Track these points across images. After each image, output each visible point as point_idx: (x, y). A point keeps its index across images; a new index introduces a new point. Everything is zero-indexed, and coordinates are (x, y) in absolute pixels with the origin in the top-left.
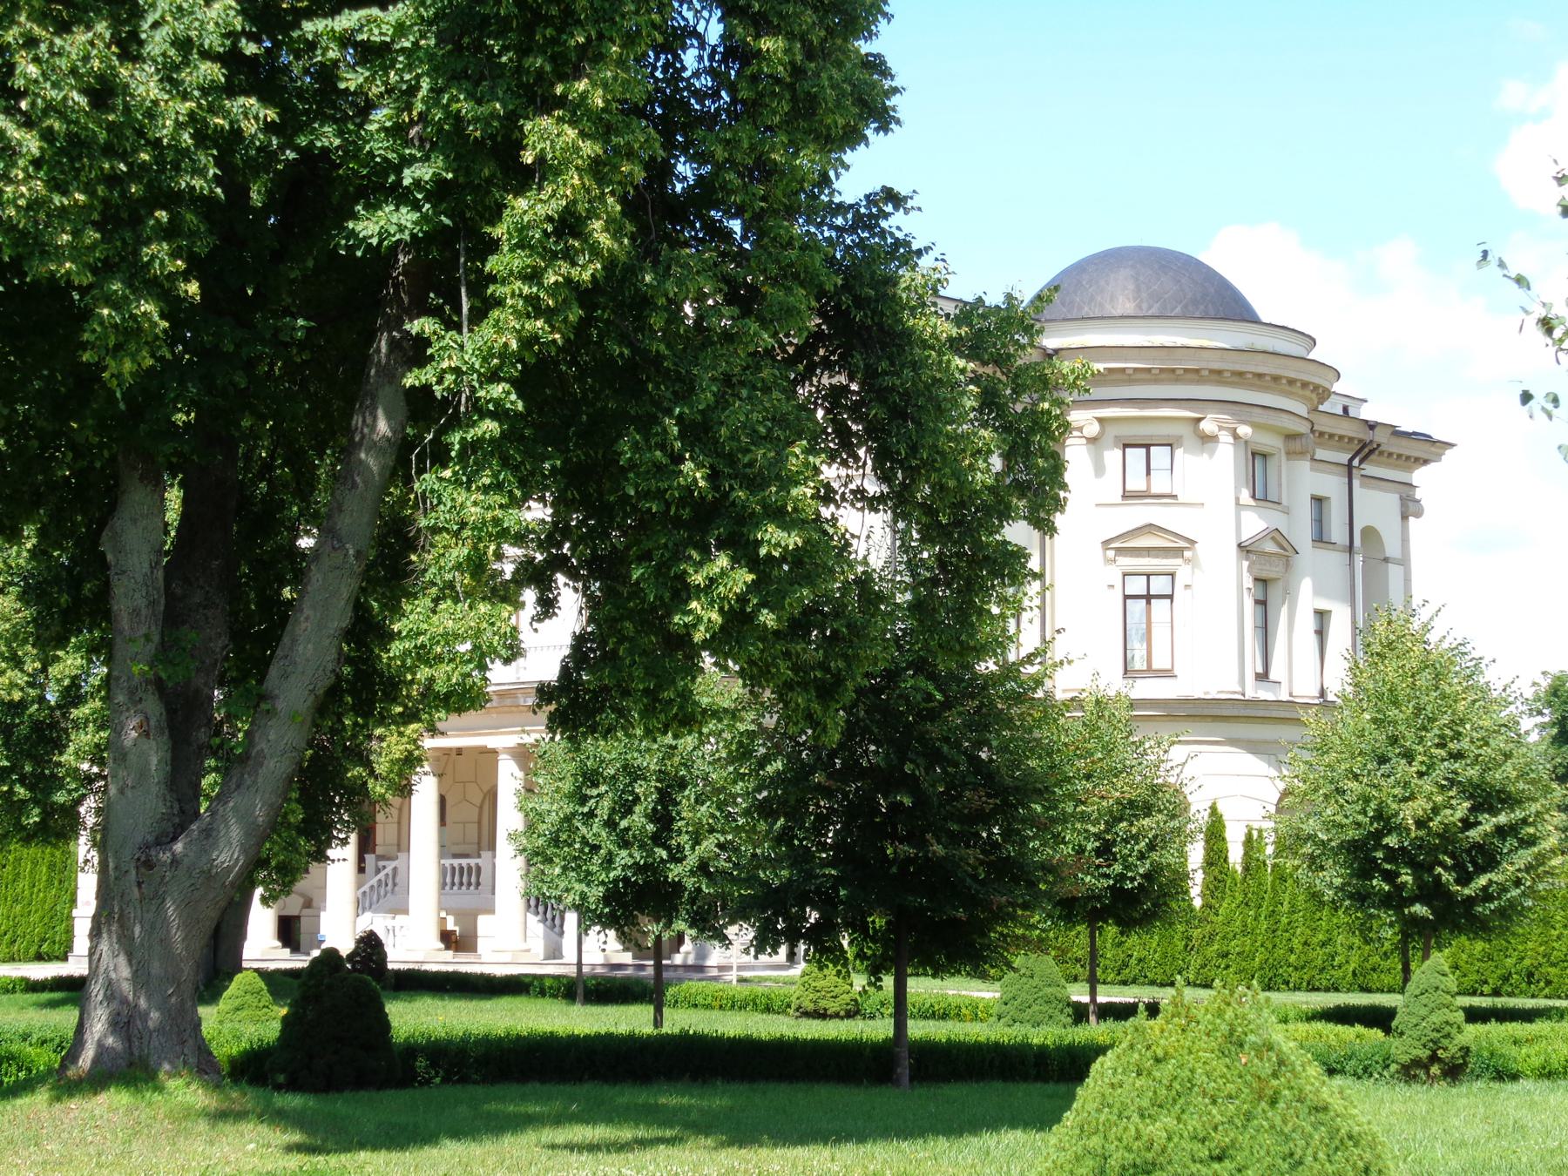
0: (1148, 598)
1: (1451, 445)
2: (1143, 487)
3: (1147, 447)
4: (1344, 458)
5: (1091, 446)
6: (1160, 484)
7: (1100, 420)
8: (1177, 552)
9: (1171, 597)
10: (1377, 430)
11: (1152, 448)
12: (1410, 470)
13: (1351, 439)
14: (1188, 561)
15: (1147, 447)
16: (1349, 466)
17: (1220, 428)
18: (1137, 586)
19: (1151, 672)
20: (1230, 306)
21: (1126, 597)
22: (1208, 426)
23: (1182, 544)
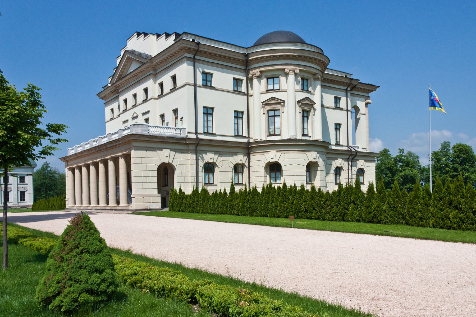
0: (274, 116)
3: (273, 78)
5: (259, 79)
6: (277, 87)
7: (260, 72)
8: (280, 103)
10: (353, 80)
11: (275, 79)
12: (368, 93)
13: (346, 83)
14: (282, 106)
15: (273, 78)
17: (290, 71)
18: (271, 113)
19: (275, 135)
21: (269, 116)
22: (286, 70)
23: (281, 101)
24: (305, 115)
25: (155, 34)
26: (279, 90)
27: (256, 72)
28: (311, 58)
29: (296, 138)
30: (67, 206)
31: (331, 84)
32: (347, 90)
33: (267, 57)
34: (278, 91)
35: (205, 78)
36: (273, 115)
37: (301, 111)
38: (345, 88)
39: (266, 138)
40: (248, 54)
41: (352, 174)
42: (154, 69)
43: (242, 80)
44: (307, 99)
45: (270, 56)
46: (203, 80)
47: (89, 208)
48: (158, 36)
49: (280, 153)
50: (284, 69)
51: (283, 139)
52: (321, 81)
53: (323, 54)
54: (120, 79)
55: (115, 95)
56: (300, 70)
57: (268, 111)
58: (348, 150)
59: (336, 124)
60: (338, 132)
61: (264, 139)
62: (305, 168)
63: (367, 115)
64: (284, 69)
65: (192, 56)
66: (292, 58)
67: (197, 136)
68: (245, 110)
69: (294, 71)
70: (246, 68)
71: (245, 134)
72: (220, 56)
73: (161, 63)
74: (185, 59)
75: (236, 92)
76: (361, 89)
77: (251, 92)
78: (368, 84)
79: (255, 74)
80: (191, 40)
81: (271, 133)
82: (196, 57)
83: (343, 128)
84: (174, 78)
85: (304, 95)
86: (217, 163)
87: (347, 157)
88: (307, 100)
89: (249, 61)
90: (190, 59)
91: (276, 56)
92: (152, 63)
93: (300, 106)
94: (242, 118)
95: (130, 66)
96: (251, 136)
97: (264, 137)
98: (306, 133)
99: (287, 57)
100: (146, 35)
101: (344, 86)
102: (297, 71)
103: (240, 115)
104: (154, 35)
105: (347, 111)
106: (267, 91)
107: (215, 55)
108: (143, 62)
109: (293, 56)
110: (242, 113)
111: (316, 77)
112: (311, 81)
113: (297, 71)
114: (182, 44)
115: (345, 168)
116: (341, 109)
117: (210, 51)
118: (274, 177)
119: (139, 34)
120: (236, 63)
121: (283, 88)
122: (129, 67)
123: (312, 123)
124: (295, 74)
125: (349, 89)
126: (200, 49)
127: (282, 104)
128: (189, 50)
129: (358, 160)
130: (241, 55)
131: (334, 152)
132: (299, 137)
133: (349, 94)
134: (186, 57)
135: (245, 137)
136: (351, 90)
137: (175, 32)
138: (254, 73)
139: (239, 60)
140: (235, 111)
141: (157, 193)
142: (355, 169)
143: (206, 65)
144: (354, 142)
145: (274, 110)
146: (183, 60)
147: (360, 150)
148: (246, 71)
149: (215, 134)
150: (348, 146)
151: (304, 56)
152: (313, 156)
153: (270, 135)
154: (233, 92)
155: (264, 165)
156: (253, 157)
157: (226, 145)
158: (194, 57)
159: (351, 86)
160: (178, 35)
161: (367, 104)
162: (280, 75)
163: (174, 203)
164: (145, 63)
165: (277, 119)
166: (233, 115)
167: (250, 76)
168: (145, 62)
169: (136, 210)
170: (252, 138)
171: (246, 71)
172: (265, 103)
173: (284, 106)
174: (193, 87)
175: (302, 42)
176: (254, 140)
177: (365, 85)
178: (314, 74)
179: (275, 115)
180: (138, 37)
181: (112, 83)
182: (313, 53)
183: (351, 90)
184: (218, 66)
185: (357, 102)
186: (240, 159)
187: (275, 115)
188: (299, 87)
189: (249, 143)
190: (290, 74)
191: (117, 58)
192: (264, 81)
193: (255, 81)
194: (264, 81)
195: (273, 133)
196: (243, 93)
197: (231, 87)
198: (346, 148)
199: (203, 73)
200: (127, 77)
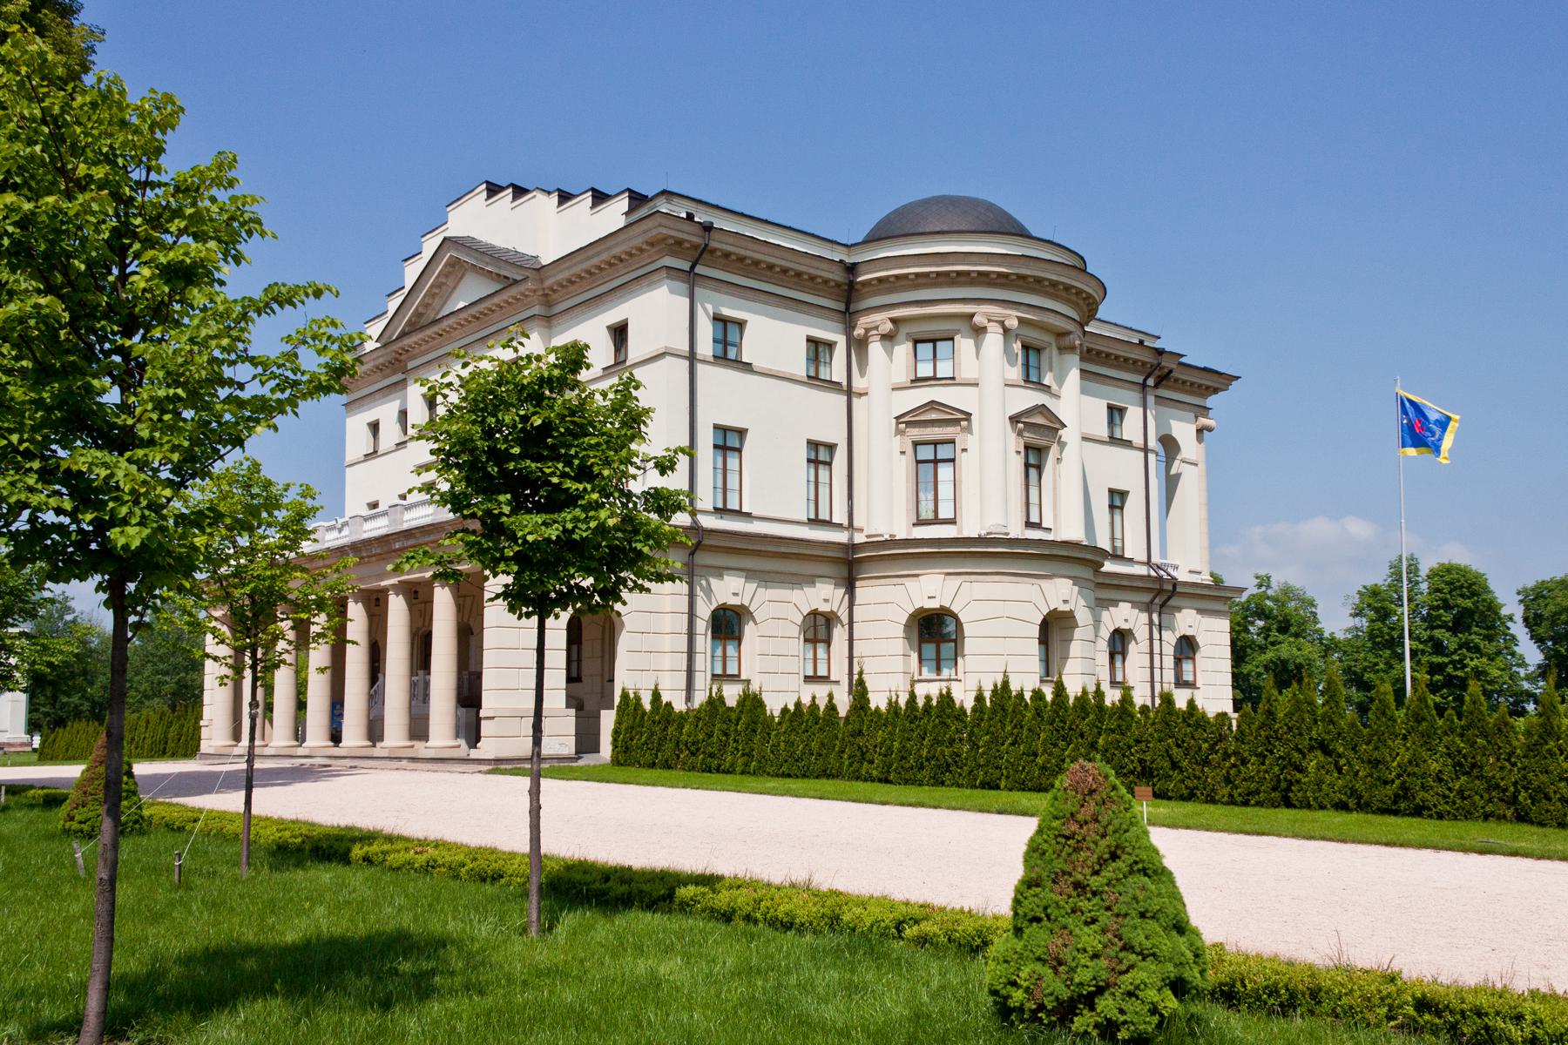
0: (936, 461)
1: (1238, 378)
2: (931, 374)
3: (934, 341)
4: (1140, 379)
5: (887, 343)
6: (944, 370)
7: (893, 321)
8: (956, 422)
9: (953, 460)
11: (939, 344)
12: (1205, 396)
13: (1144, 364)
14: (964, 430)
15: (934, 341)
16: (1144, 385)
17: (989, 321)
18: (926, 453)
19: (936, 521)
20: (1014, 230)
22: (978, 320)
23: (960, 416)
24: (1034, 458)
25: (507, 187)
26: (953, 378)
27: (881, 320)
28: (1054, 284)
29: (1007, 534)
30: (205, 747)
31: (1097, 363)
32: (1144, 385)
33: (917, 275)
34: (951, 380)
35: (720, 336)
37: (1022, 449)
38: (1140, 379)
39: (909, 532)
40: (855, 264)
41: (1161, 654)
42: (547, 301)
43: (830, 346)
44: (1042, 409)
45: (927, 275)
46: (715, 341)
47: (300, 751)
48: (564, 197)
49: (957, 580)
50: (972, 316)
51: (966, 534)
52: (1082, 359)
53: (1084, 271)
54: (414, 327)
55: (388, 376)
56: (1021, 320)
57: (916, 444)
58: (1149, 576)
59: (1112, 492)
60: (1117, 518)
62: (1036, 632)
63: (1202, 466)
64: (972, 316)
65: (686, 266)
66: (998, 281)
67: (695, 522)
68: (838, 436)
69: (1002, 323)
70: (847, 308)
71: (840, 517)
72: (771, 267)
73: (573, 283)
74: (664, 273)
75: (814, 380)
76: (1184, 382)
77: (858, 383)
78: (1205, 370)
79: (876, 328)
80: (684, 215)
81: (924, 516)
82: (699, 269)
83: (1134, 505)
84: (619, 333)
85: (1032, 398)
86: (752, 609)
87: (1146, 598)
88: (1041, 413)
89: (858, 287)
90: (680, 274)
91: (947, 274)
92: (542, 281)
93: (1020, 434)
94: (829, 464)
95: (455, 288)
96: (856, 524)
97: (902, 529)
98: (1034, 519)
99: (984, 279)
100: (519, 192)
101: (1136, 371)
102: (1013, 323)
103: (823, 455)
104: (549, 193)
105: (1146, 450)
106: (912, 381)
107: (756, 263)
108: (506, 277)
109: (999, 275)
110: (831, 448)
111: (1066, 341)
112: (1051, 353)
113: (1013, 323)
114: (660, 225)
115: (1141, 632)
116: (1127, 444)
117: (743, 252)
118: (934, 656)
119: (493, 190)
120: (815, 291)
121: (966, 373)
122: (452, 292)
123: (1055, 489)
124: (1006, 331)
125: (1151, 382)
126: (713, 244)
127: (964, 423)
128: (676, 247)
129: (1179, 609)
130: (835, 268)
131: (1107, 581)
132: (1017, 530)
133: (1151, 399)
134: (668, 268)
135: (840, 526)
136: (1156, 386)
137: (629, 190)
138: (873, 325)
139: (826, 282)
140: (810, 442)
141: (563, 704)
142: (1170, 638)
143: (726, 293)
144: (1163, 553)
145: (935, 443)
146: (655, 277)
147: (1182, 576)
148: (847, 317)
149: (748, 515)
150: (1148, 563)
151: (1017, 275)
152: (1061, 592)
153: (920, 523)
154: (806, 380)
155: (904, 619)
156: (863, 591)
157: (783, 550)
158: (693, 267)
159: (1157, 373)
160: (637, 200)
161: (1200, 431)
162: (957, 332)
163: (632, 739)
164: (516, 282)
165: (945, 471)
166: (803, 453)
167: (859, 332)
168: (519, 278)
169: (498, 761)
170: (861, 530)
171: (847, 317)
172: (906, 419)
173: (969, 430)
174: (687, 363)
175: (1022, 233)
176: (868, 537)
177: (1196, 373)
178: (1061, 334)
180: (489, 197)
181: (384, 340)
182: (1059, 268)
183: (1156, 386)
184: (763, 297)
185: (1172, 422)
186: (825, 595)
188: (1015, 373)
189: (852, 547)
190: (989, 330)
191: (406, 260)
192: (903, 350)
193: (876, 349)
194: (903, 350)
195: (931, 516)
196: (833, 386)
197: (798, 365)
198: (1142, 570)
199: (718, 319)
200: (445, 324)
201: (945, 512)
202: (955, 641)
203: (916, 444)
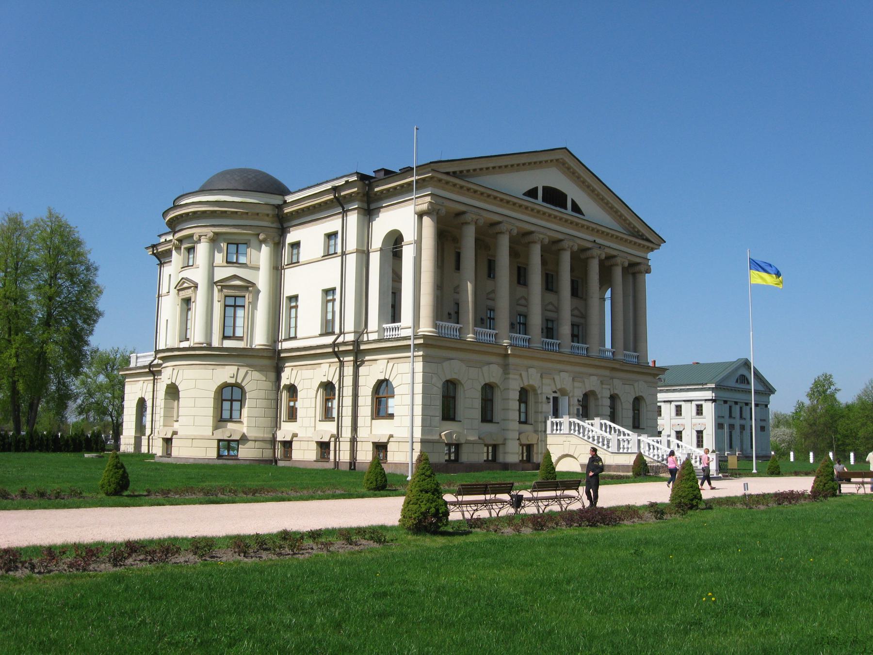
3: (237, 244)
6: (242, 260)
9: (244, 306)
14: (250, 292)
15: (237, 244)
18: (231, 301)
19: (233, 337)
22: (261, 237)
34: (244, 266)
36: (233, 304)
51: (249, 347)
57: (226, 296)
61: (217, 346)
121: (253, 263)
145: (235, 297)
179: (237, 304)
187: (237, 304)
201: (239, 333)
202: (241, 401)
203: (226, 296)
